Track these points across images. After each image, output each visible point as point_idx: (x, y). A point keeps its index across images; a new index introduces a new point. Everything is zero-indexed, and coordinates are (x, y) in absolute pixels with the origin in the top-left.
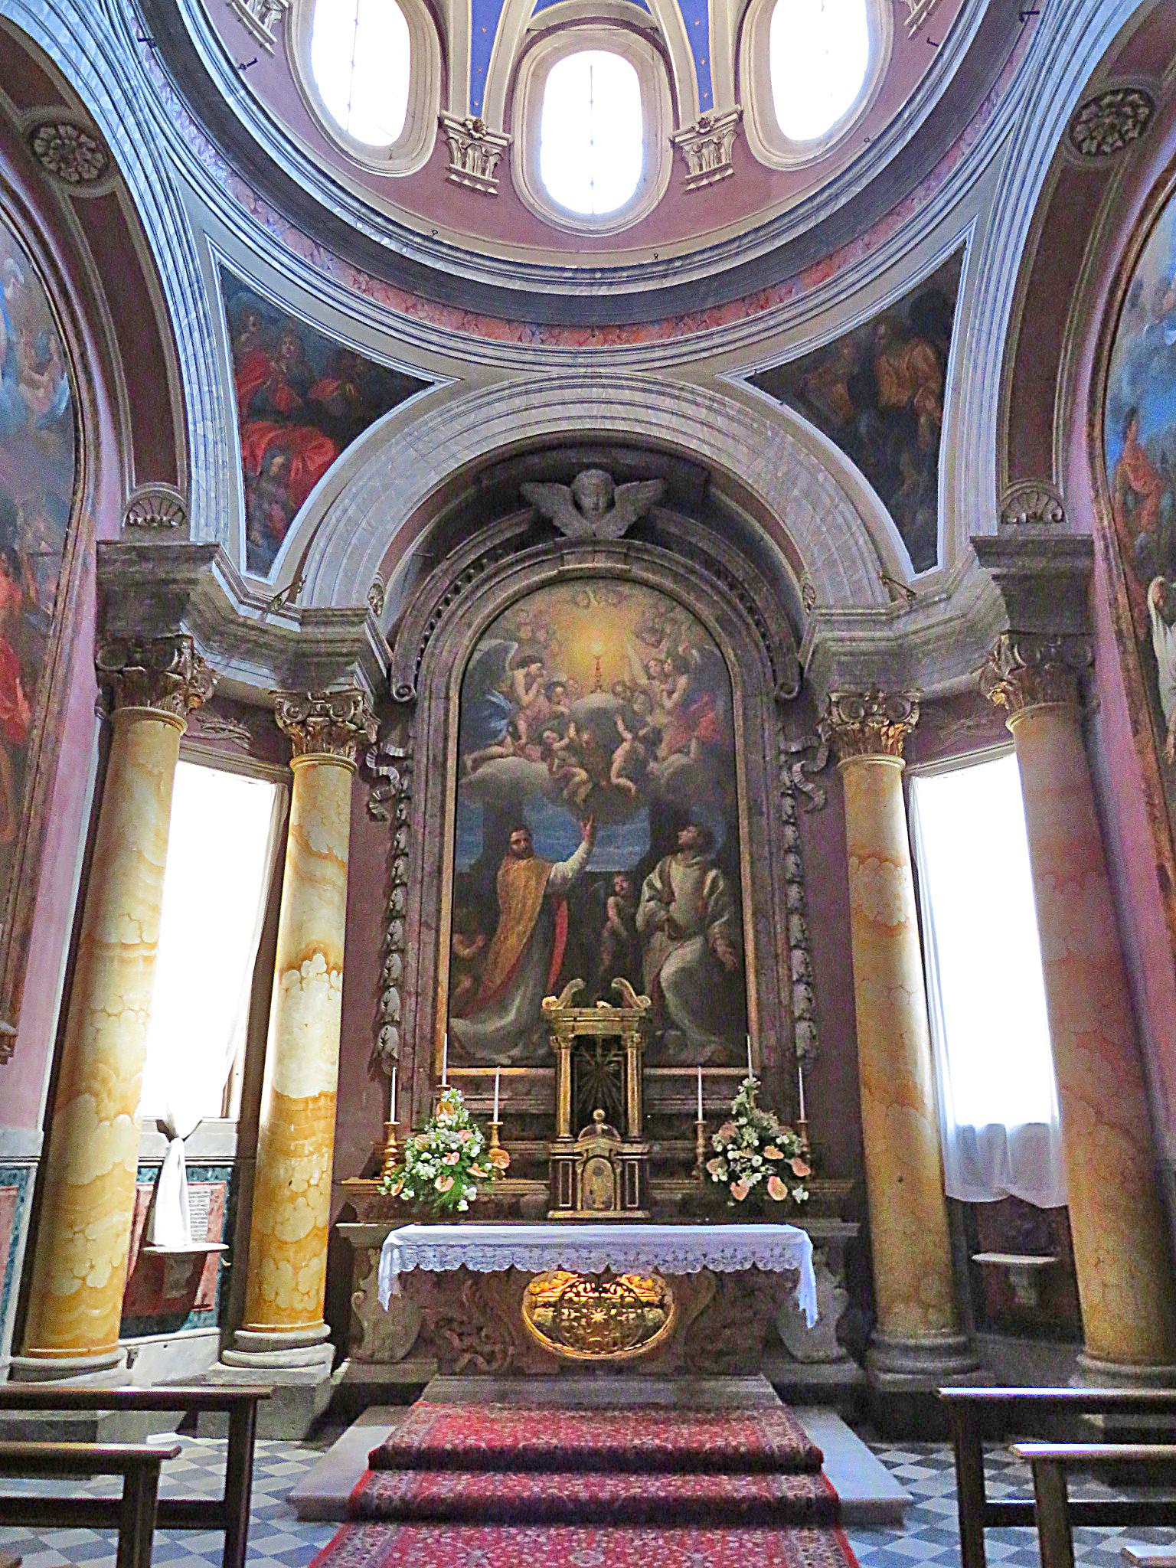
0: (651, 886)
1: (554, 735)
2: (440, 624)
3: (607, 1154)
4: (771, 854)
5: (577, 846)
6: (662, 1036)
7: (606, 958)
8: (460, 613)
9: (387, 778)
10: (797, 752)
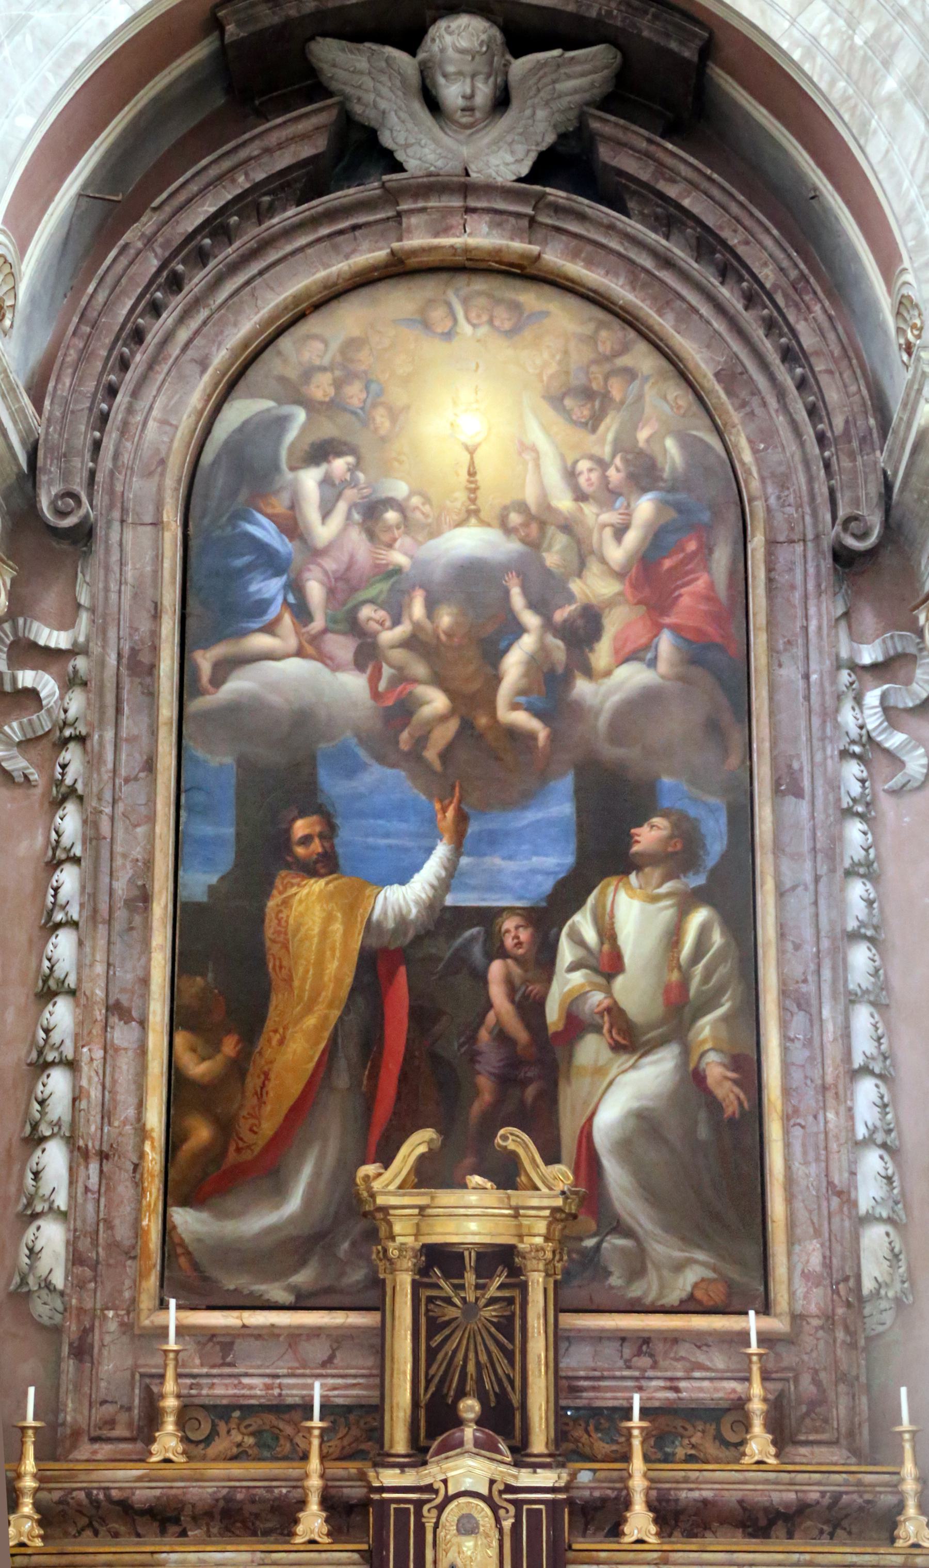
0: (578, 941)
1: (381, 614)
2: (140, 359)
3: (484, 1491)
4: (817, 879)
5: (429, 851)
6: (598, 1247)
7: (485, 1084)
8: (183, 335)
9: (32, 694)
10: (874, 667)
